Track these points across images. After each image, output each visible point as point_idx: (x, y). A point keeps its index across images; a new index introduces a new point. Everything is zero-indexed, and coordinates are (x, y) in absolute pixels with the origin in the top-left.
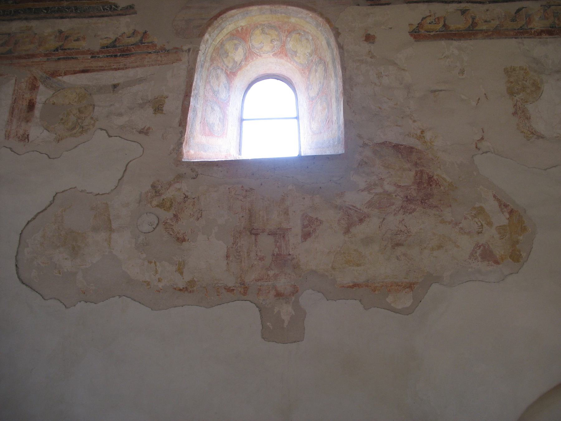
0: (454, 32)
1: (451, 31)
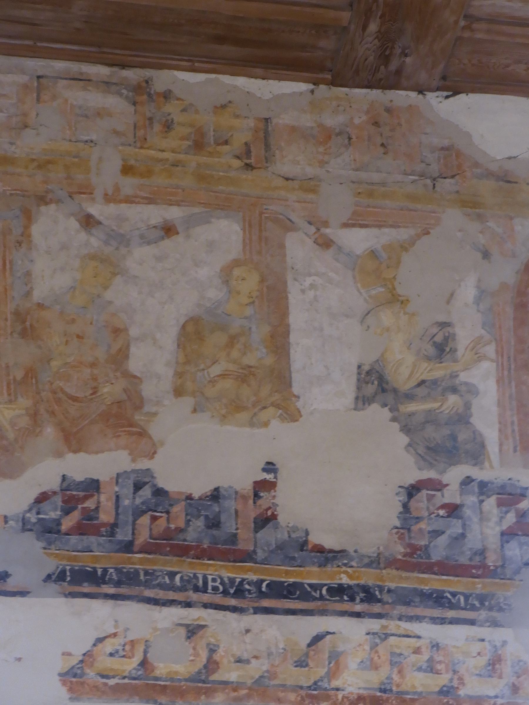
1: (157, 679)
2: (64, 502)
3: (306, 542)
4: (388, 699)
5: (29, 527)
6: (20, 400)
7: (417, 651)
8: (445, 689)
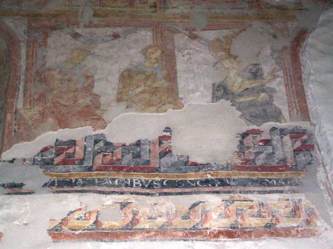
0: (106, 231)
1: (103, 229)
2: (56, 151)
3: (188, 161)
4: (236, 232)
5: (37, 163)
6: (36, 107)
7: (251, 207)
8: (268, 225)
